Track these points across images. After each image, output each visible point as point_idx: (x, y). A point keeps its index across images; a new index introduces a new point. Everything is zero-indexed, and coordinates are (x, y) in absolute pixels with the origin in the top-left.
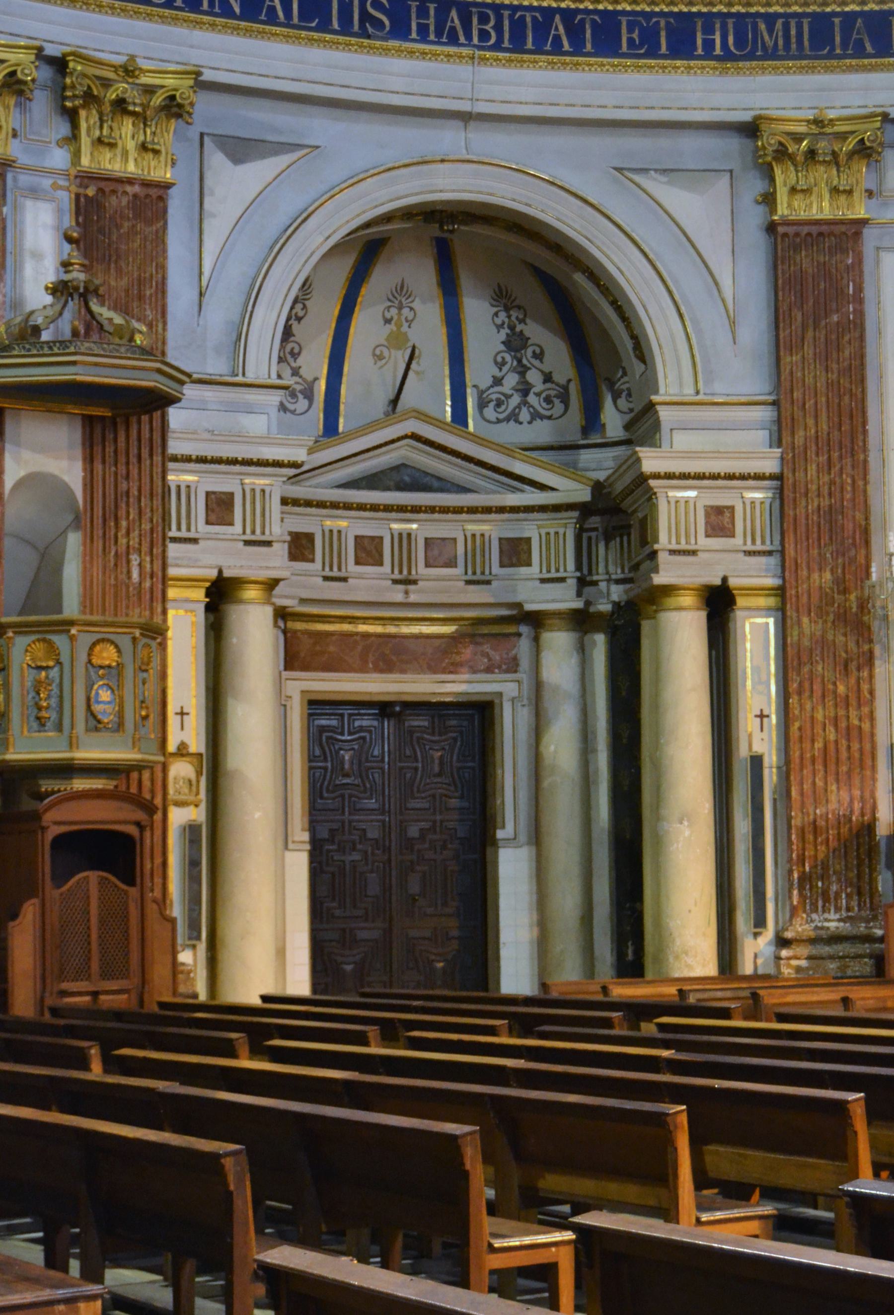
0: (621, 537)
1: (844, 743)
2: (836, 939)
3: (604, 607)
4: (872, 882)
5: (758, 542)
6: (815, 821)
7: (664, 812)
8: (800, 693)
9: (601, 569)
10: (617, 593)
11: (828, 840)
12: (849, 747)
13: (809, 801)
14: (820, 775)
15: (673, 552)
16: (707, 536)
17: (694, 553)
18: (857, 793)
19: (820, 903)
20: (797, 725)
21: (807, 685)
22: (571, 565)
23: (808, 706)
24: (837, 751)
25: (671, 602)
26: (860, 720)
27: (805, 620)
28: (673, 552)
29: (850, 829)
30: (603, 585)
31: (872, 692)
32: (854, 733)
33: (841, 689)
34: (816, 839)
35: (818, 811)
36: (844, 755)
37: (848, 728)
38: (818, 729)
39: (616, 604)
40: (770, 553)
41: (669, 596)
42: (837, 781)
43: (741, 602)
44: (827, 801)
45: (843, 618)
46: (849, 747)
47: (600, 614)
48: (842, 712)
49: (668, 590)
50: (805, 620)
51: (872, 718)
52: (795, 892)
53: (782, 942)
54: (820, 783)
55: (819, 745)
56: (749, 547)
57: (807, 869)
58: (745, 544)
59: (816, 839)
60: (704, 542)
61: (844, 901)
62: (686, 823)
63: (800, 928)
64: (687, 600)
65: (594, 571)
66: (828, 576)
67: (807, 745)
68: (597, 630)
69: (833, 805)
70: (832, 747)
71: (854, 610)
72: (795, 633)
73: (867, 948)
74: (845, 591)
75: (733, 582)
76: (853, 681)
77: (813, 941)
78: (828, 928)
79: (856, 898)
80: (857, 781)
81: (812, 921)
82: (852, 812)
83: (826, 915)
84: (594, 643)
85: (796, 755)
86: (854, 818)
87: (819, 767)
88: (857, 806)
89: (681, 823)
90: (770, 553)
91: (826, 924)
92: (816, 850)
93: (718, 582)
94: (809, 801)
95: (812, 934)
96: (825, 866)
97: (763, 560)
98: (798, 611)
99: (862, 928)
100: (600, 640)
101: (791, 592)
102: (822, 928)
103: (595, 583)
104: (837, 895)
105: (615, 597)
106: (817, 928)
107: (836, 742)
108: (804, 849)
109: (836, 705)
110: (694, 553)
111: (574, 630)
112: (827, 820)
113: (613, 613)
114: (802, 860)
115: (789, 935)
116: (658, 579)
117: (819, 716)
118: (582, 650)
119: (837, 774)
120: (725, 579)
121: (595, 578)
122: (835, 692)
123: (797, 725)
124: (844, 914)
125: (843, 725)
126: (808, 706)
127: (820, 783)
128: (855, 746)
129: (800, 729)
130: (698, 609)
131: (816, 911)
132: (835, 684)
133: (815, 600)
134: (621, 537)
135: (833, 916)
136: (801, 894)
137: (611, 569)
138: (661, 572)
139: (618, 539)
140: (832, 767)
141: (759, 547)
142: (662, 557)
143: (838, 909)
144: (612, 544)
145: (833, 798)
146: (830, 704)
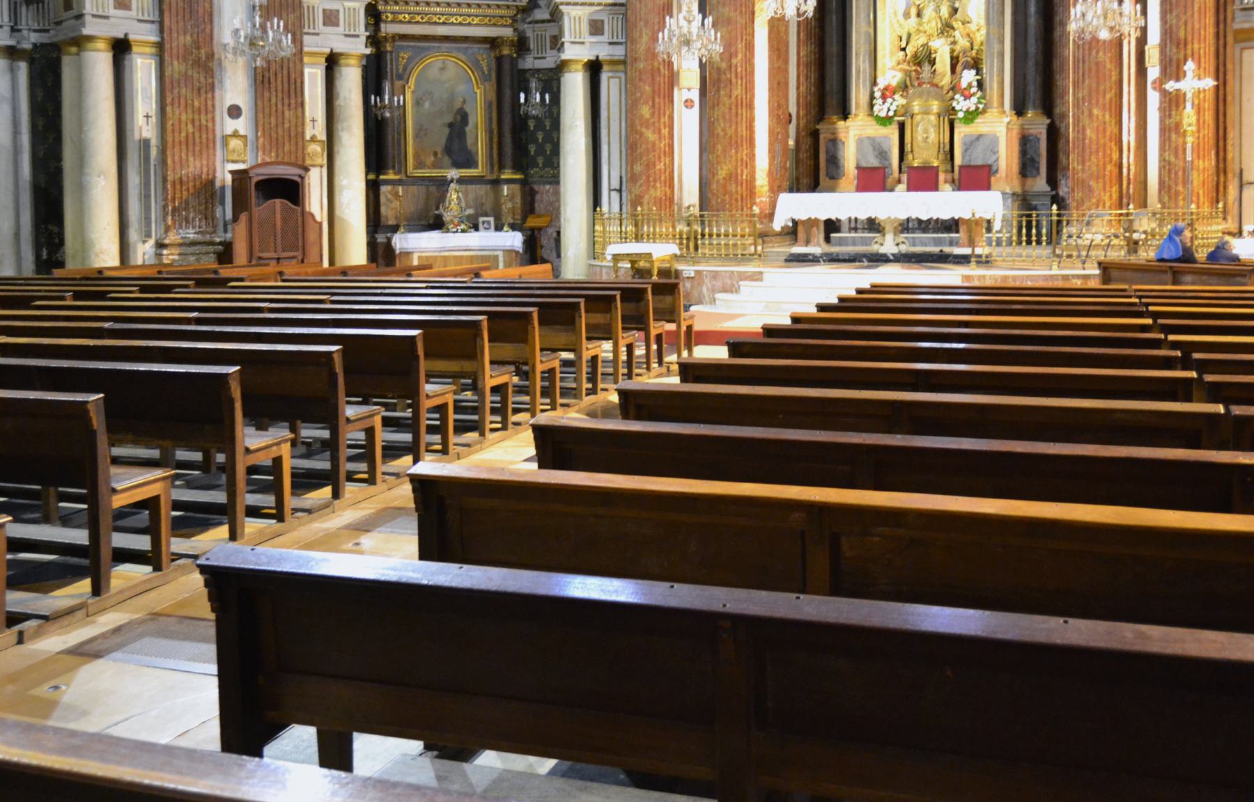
0: (38, 3)
1: (197, 135)
2: (193, 243)
3: (27, 46)
4: (213, 211)
5: (146, 14)
6: (181, 178)
7: (87, 171)
8: (172, 104)
9: (23, 22)
10: (34, 38)
11: (188, 188)
12: (200, 137)
13: (178, 166)
14: (184, 151)
15: (94, 16)
16: (115, 8)
17: (107, 17)
18: (205, 162)
19: (184, 224)
20: (171, 122)
21: (176, 100)
22: (6, 18)
23: (177, 112)
24: (194, 139)
25: (90, 45)
26: (207, 121)
27: (176, 63)
28: (94, 16)
29: (201, 183)
30: (25, 33)
31: (213, 106)
32: (204, 129)
33: (196, 103)
34: (181, 187)
35: (183, 172)
36: (197, 140)
37: (200, 125)
38: (183, 126)
39: (35, 45)
40: (153, 22)
41: (92, 42)
42: (194, 155)
43: (135, 49)
44: (188, 166)
45: (197, 63)
46: (200, 137)
47: (24, 51)
48: (196, 117)
49: (90, 38)
50: (176, 63)
51: (213, 120)
52: (170, 218)
53: (160, 245)
54: (184, 156)
55: (183, 134)
56: (140, 17)
57: (177, 204)
58: (138, 15)
59: (181, 187)
60: (112, 11)
61: (198, 223)
62: (102, 177)
63: (172, 238)
64: (101, 45)
65: (19, 23)
66: (188, 38)
67: (176, 134)
68: (22, 59)
69: (191, 169)
70: (190, 136)
71: (204, 58)
72: (170, 70)
73: (211, 248)
74: (198, 48)
75: (131, 37)
76: (203, 99)
77: (180, 245)
78: (189, 238)
79: (204, 221)
80: (205, 156)
81: (180, 234)
82: (202, 173)
83: (187, 231)
84: (19, 68)
85: (170, 139)
86: (203, 176)
87: (184, 147)
88: (205, 170)
89: (99, 177)
90: (153, 22)
91: (188, 236)
92: (182, 194)
93: (121, 36)
94: (178, 166)
95: (181, 241)
96: (187, 203)
97: (149, 26)
98: (171, 57)
99: (208, 237)
100: (23, 67)
101: (167, 46)
102: (185, 238)
103: (19, 31)
104: (193, 219)
105: (33, 40)
106: (182, 238)
107: (193, 133)
108: (175, 193)
109: (193, 112)
110: (107, 17)
111: (8, 58)
112: (188, 177)
113: (32, 50)
114: (174, 199)
115: (167, 241)
116: (86, 31)
117: (184, 117)
118: (13, 71)
119: (194, 151)
120: (126, 35)
121: (20, 27)
122: (193, 105)
123: (171, 122)
124: (197, 230)
125: (197, 123)
126: (177, 112)
127: (184, 156)
128: (204, 136)
129: (173, 125)
130: (109, 51)
131: (181, 227)
132: (192, 100)
133: (181, 51)
134: (38, 3)
135: (191, 231)
136: (172, 219)
137: (30, 22)
138: (87, 28)
139: (35, 5)
140: (191, 148)
141: (146, 18)
142: (88, 18)
143: (194, 227)
144: (31, 7)
145: (191, 165)
146: (190, 111)
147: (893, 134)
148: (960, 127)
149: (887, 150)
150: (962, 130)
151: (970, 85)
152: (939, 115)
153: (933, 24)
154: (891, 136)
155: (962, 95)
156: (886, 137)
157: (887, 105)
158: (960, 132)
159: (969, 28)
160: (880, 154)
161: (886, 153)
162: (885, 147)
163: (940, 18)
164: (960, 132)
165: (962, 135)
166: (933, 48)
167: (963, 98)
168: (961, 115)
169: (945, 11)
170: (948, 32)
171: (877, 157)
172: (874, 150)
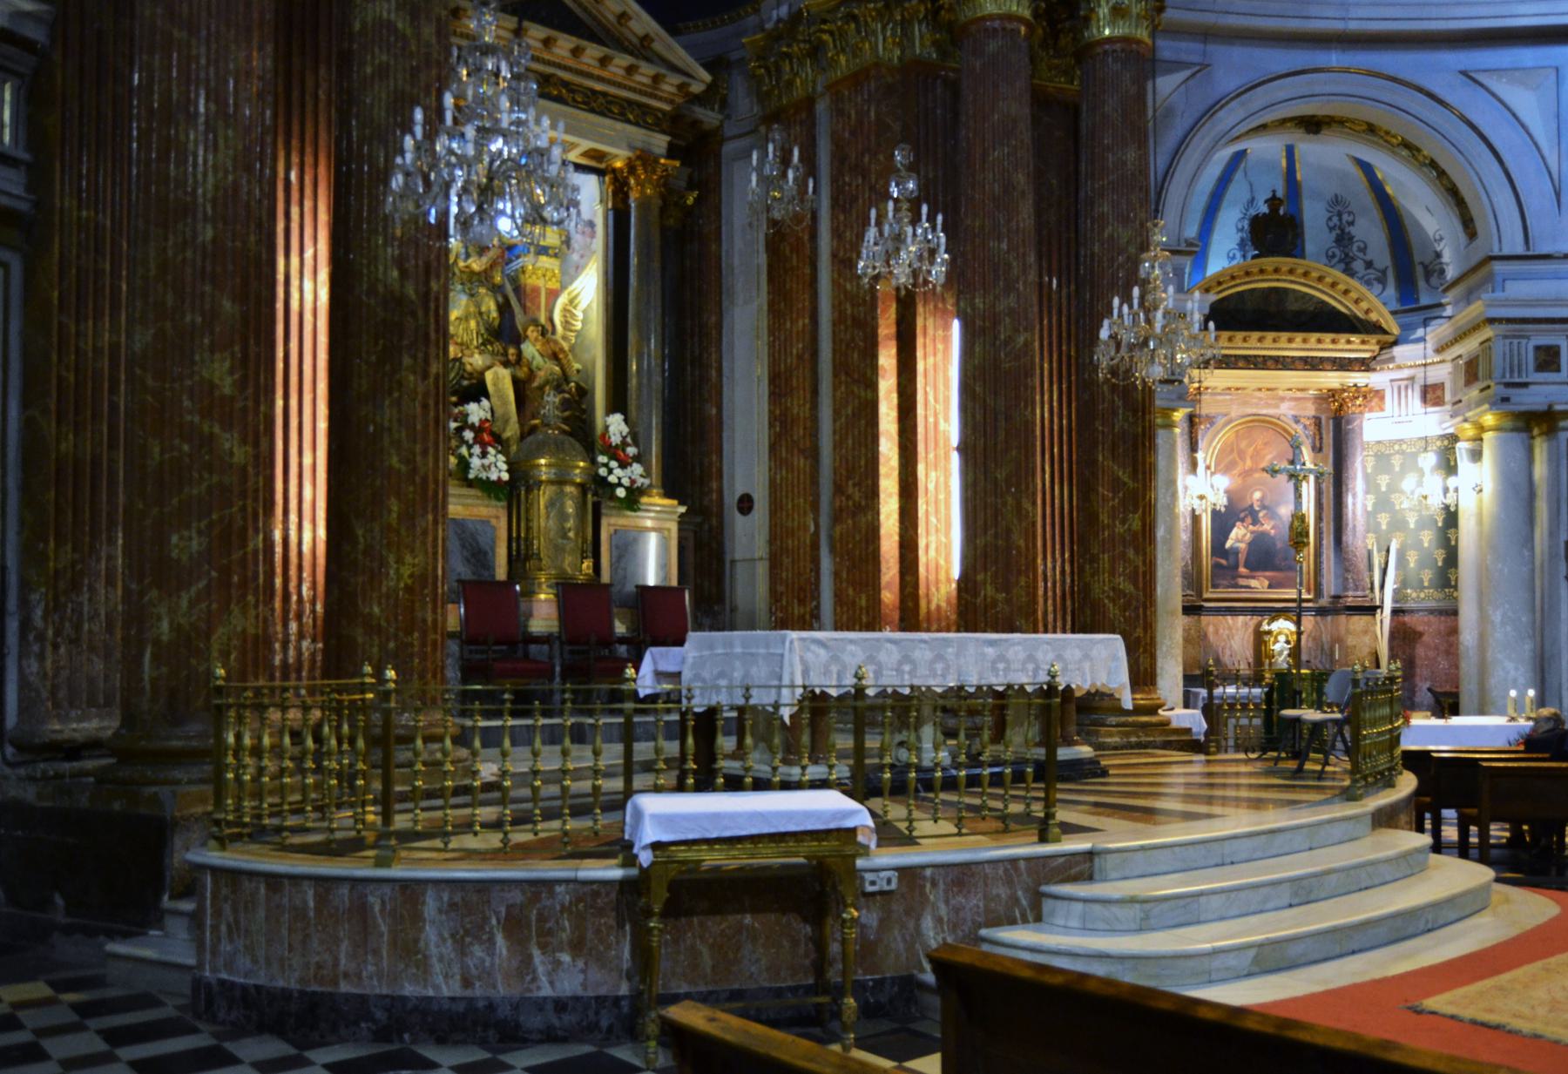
147: (497, 517)
148: (611, 516)
149: (487, 548)
150: (613, 520)
151: (624, 444)
152: (583, 487)
153: (473, 324)
154: (493, 522)
155: (613, 457)
156: (485, 522)
157: (491, 459)
158: (609, 525)
159: (556, 342)
160: (473, 555)
161: (486, 553)
162: (483, 541)
163: (481, 314)
164: (609, 525)
165: (612, 529)
166: (468, 368)
167: (614, 464)
168: (621, 493)
169: (490, 306)
170: (492, 344)
171: (468, 561)
172: (463, 546)
